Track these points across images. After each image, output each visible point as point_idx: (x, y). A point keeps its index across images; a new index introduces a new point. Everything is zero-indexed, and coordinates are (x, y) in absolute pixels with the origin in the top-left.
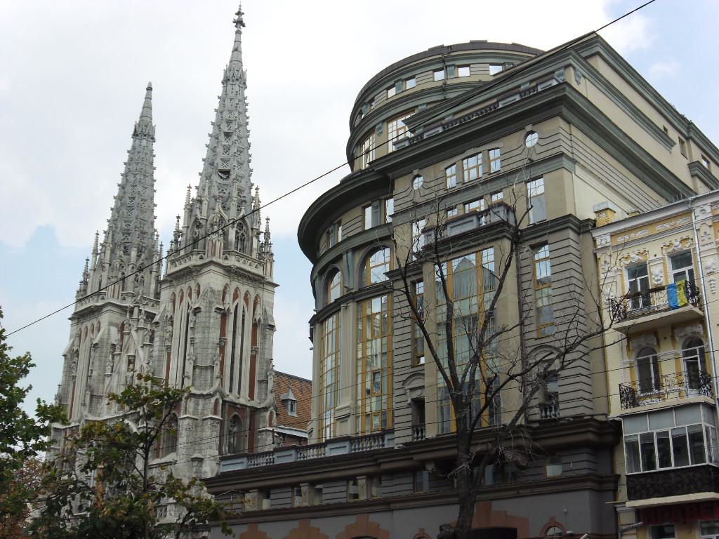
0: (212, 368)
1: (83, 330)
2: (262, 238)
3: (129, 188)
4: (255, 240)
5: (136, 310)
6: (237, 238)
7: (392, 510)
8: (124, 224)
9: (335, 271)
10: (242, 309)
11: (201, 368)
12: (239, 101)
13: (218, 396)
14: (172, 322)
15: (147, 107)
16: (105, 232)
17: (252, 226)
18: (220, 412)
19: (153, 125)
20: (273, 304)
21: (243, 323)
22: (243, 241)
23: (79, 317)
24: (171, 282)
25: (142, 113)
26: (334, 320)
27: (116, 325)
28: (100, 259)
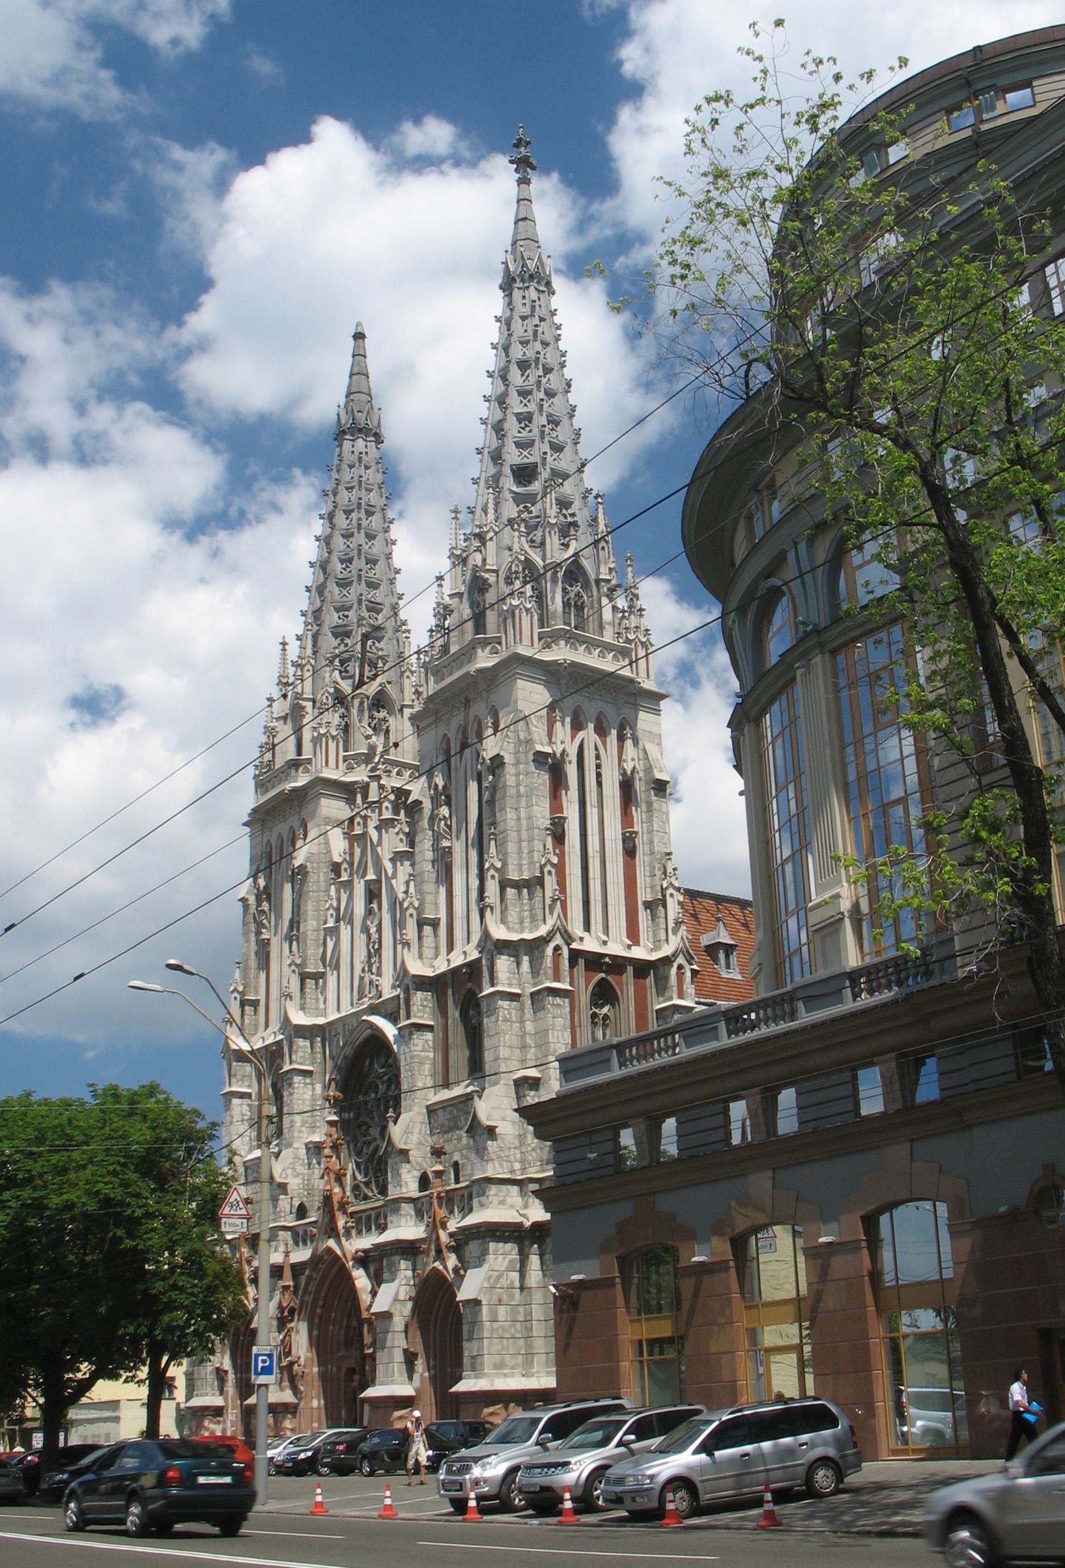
0: (540, 882)
1: (274, 844)
3: (339, 543)
5: (374, 786)
6: (567, 604)
7: (970, 1127)
8: (336, 615)
9: (775, 595)
10: (593, 753)
11: (518, 885)
12: (542, 319)
13: (558, 940)
14: (448, 797)
15: (358, 372)
17: (598, 573)
18: (567, 974)
20: (660, 736)
21: (599, 784)
22: (580, 608)
23: (261, 818)
25: (350, 385)
26: (785, 706)
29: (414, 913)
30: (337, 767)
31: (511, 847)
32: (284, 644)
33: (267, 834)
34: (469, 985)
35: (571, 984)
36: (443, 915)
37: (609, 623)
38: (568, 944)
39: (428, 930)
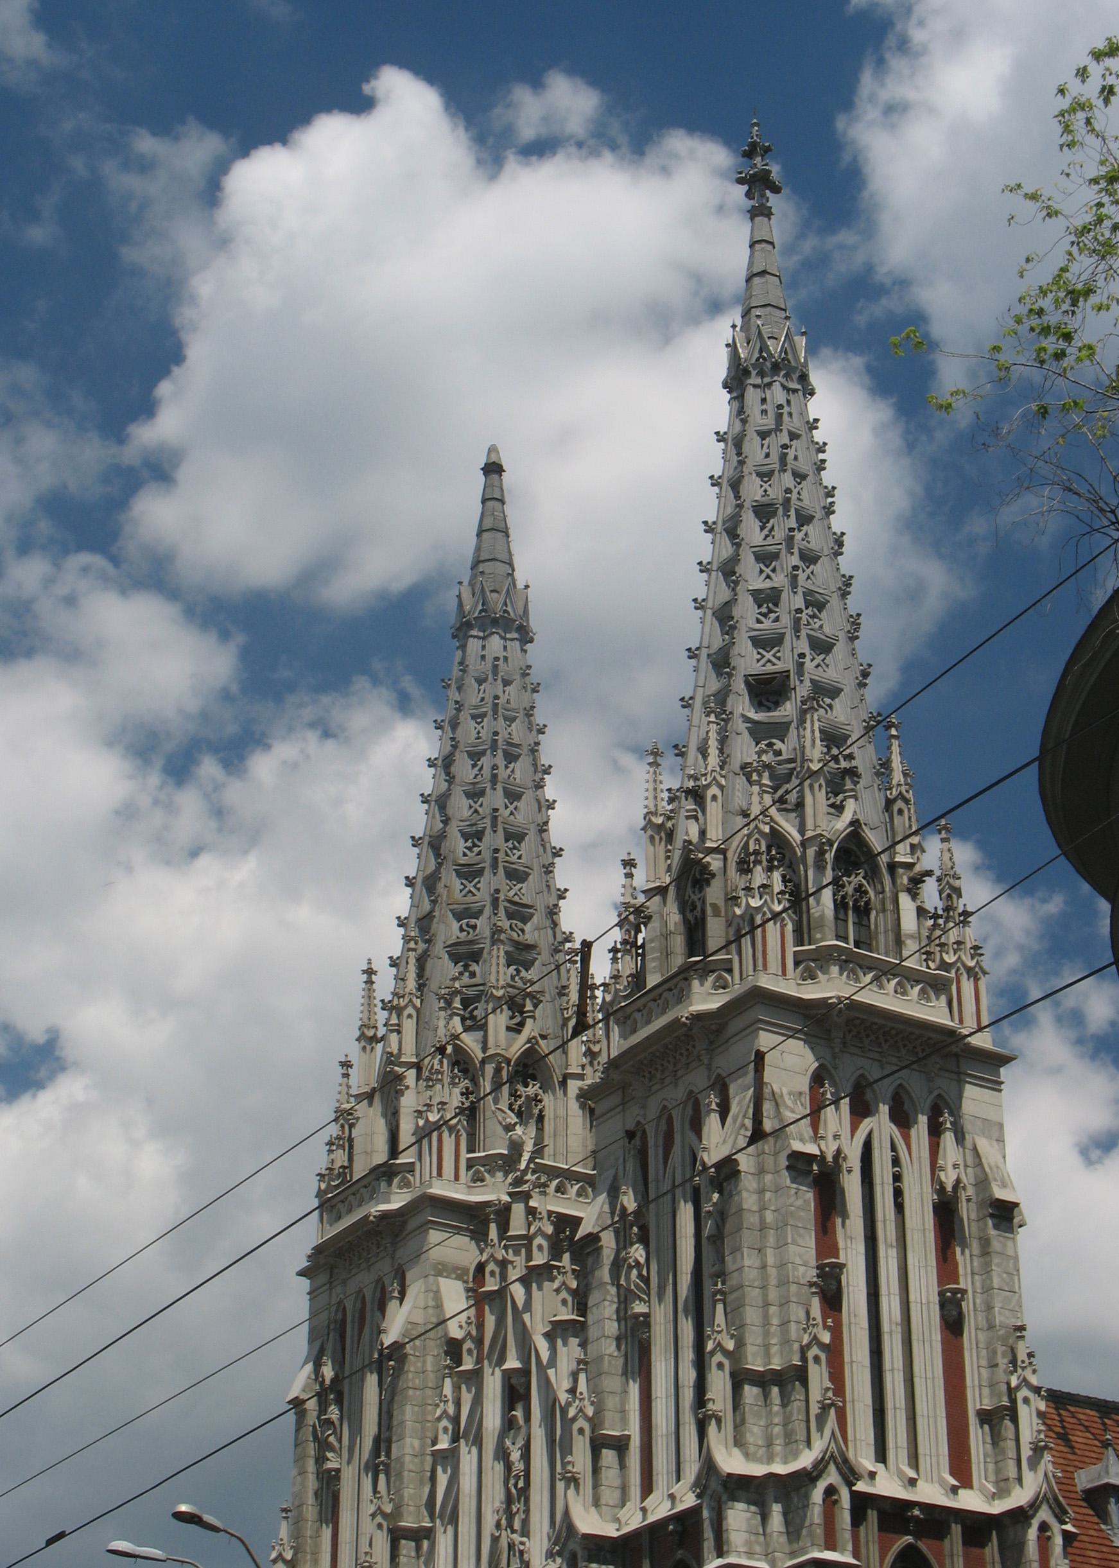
0: (801, 1375)
2: (930, 893)
3: (460, 806)
4: (907, 904)
5: (518, 1209)
6: (840, 905)
8: (455, 925)
10: (888, 1155)
11: (763, 1380)
12: (793, 436)
13: (832, 1477)
14: (644, 1229)
16: (394, 963)
18: (847, 1535)
19: (520, 585)
20: (1001, 1126)
21: (899, 1207)
22: (863, 912)
24: (624, 1087)
25: (478, 549)
27: (459, 1273)
28: (384, 1052)
29: (587, 1427)
30: (457, 1178)
31: (752, 1315)
32: (370, 972)
33: (339, 1289)
34: (680, 1554)
35: (856, 1555)
36: (634, 1430)
37: (911, 936)
38: (850, 1484)
39: (609, 1456)
